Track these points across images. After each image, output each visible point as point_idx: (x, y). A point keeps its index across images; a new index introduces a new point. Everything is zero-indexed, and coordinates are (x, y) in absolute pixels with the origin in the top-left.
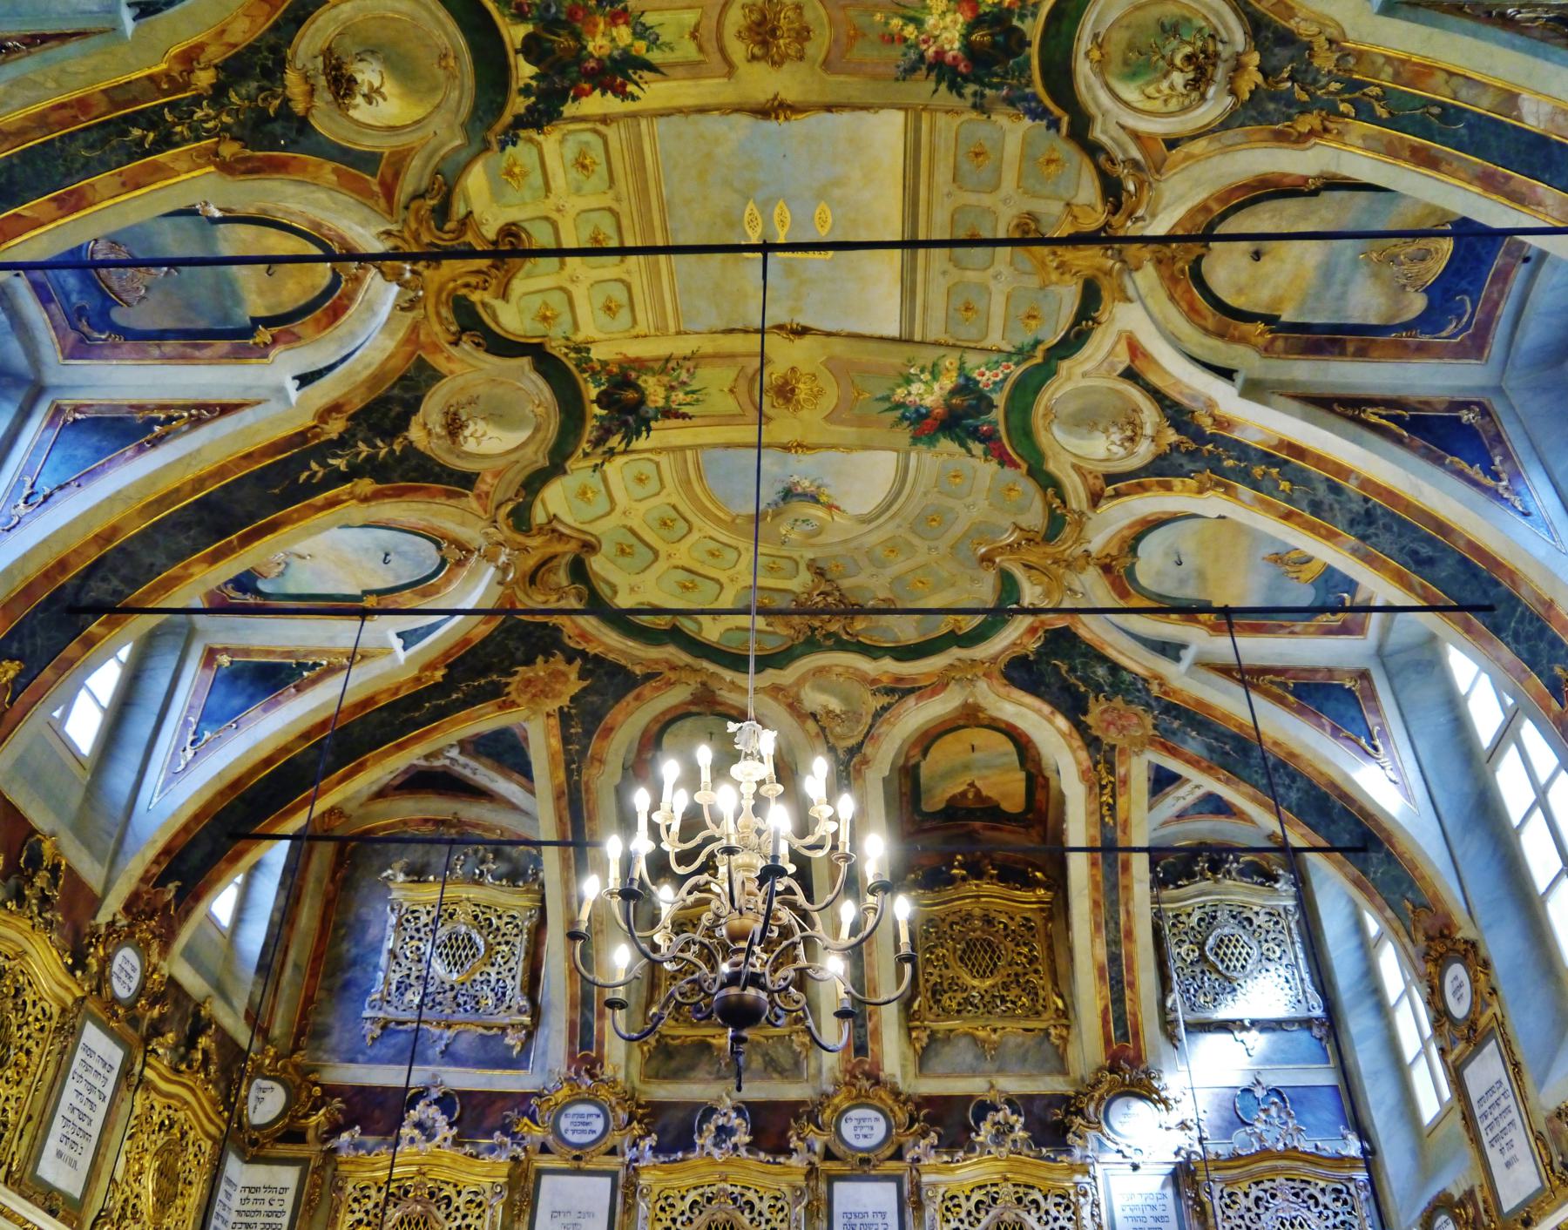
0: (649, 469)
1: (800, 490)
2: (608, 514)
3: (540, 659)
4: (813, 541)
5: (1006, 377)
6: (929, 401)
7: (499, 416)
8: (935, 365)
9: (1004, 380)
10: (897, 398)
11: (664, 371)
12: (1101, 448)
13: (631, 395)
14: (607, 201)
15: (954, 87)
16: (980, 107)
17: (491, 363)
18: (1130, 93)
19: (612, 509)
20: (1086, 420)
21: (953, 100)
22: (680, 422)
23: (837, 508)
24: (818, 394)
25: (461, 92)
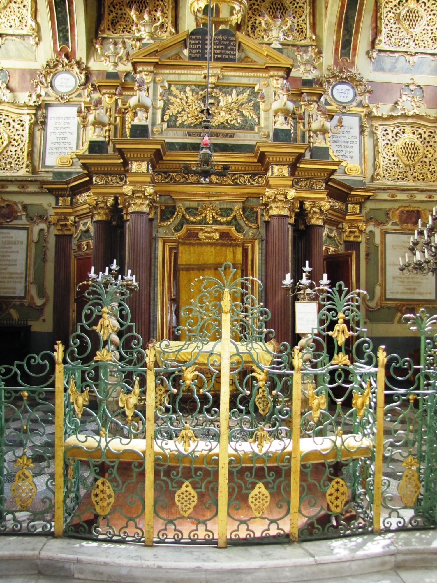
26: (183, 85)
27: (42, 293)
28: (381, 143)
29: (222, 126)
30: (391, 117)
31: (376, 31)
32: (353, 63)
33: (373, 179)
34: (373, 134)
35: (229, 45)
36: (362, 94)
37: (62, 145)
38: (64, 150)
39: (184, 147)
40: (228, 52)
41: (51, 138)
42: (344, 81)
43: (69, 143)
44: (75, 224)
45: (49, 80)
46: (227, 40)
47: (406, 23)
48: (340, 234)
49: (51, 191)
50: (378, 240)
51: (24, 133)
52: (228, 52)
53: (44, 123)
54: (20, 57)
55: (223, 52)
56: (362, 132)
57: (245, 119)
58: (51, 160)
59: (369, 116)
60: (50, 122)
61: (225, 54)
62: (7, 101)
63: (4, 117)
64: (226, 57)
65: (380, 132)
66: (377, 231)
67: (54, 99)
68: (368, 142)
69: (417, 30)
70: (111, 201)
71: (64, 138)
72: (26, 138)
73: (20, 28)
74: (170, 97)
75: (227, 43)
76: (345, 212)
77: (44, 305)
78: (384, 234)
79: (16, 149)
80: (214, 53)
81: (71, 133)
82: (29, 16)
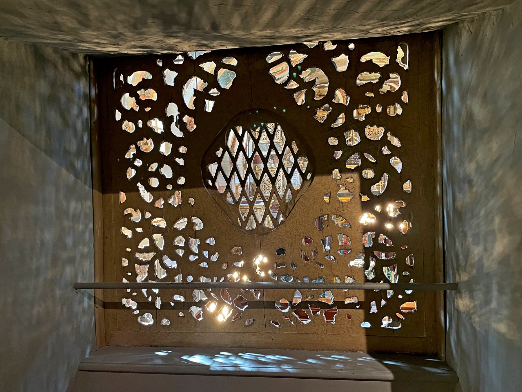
35: (357, 158)
37: (294, 182)
38: (295, 184)
40: (356, 161)
43: (297, 181)
45: (288, 158)
46: (356, 157)
51: (281, 178)
52: (356, 161)
55: (355, 161)
61: (355, 162)
62: (274, 167)
63: (273, 173)
64: (356, 163)
67: (290, 165)
71: (295, 179)
73: (276, 139)
74: (337, 177)
75: (356, 157)
79: (278, 184)
80: (352, 162)
81: (297, 177)
82: (279, 135)
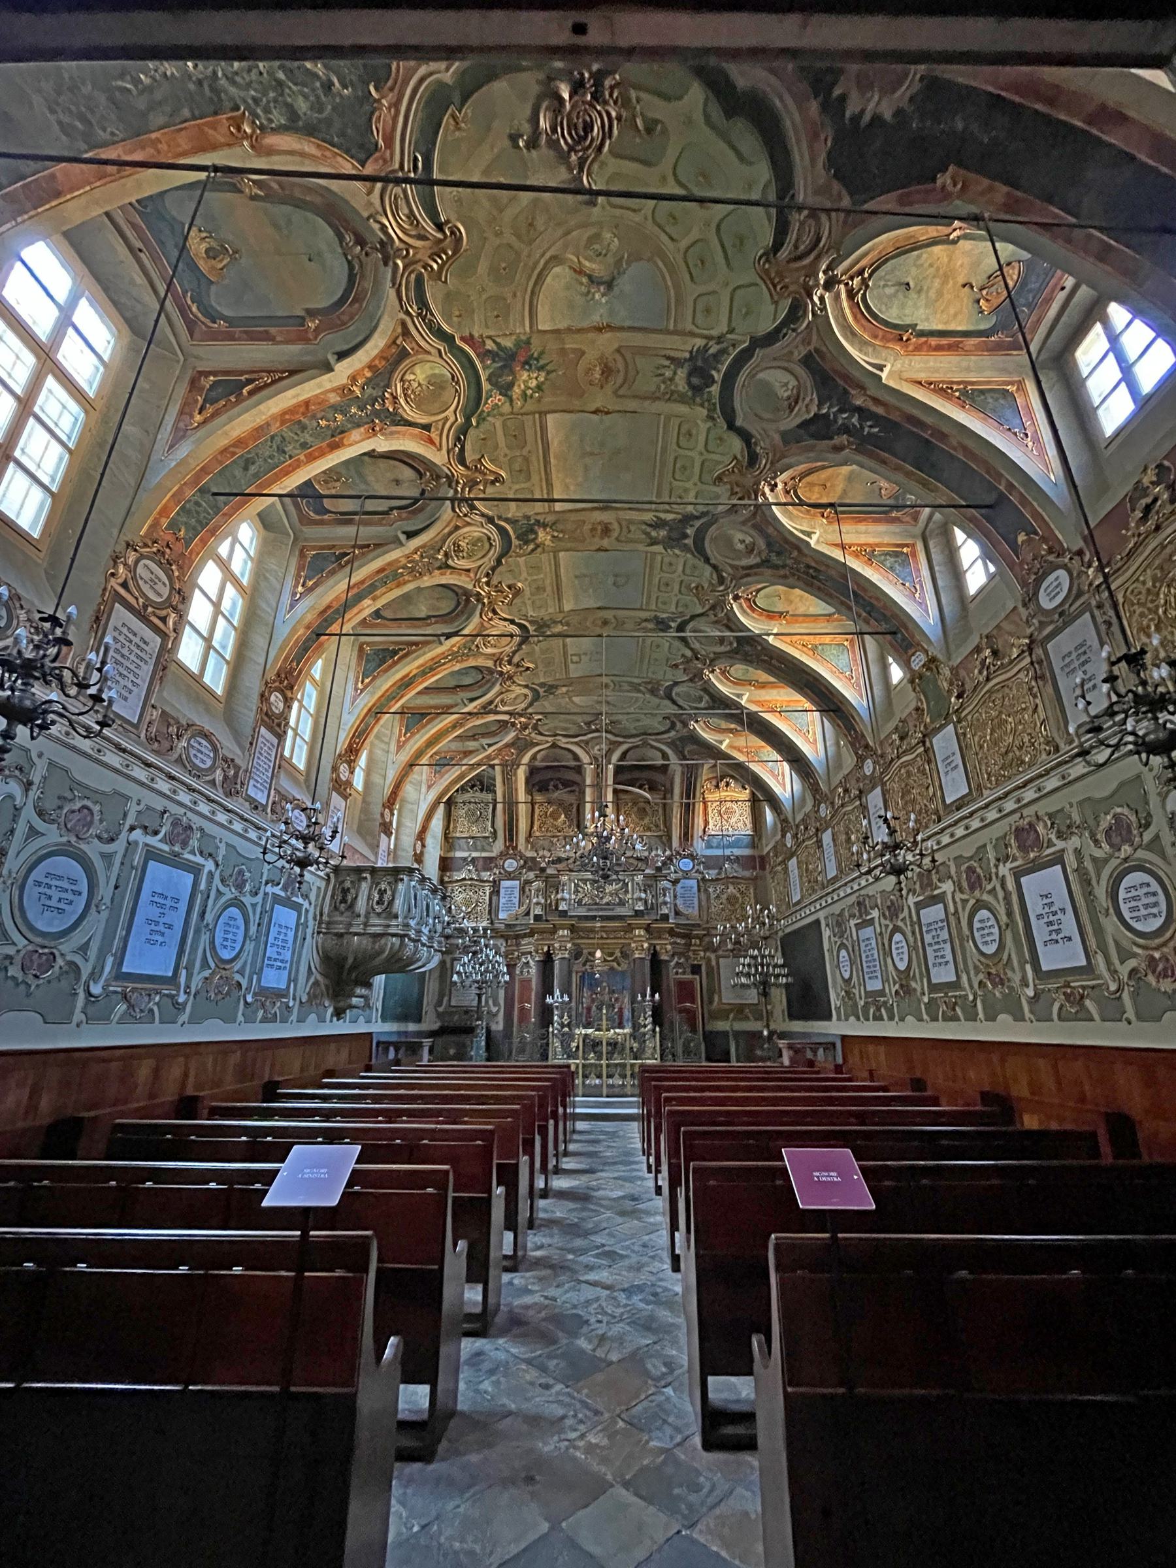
0: (700, 319)
1: (602, 288)
2: (739, 287)
3: (867, 118)
4: (591, 231)
5: (486, 403)
6: (525, 375)
7: (766, 391)
8: (526, 400)
9: (487, 399)
10: (543, 374)
11: (673, 392)
12: (419, 375)
13: (695, 381)
14: (675, 483)
15: (538, 521)
16: (528, 518)
17: (754, 429)
18: (476, 534)
19: (735, 290)
20: (437, 385)
21: (538, 517)
22: (672, 354)
23: (575, 270)
24: (589, 371)
25: (712, 531)
26: (585, 881)
27: (496, 1004)
28: (713, 896)
29: (608, 904)
30: (717, 880)
31: (706, 823)
32: (692, 845)
33: (708, 922)
34: (706, 890)
36: (699, 864)
39: (586, 918)
41: (502, 901)
42: (685, 857)
44: (519, 958)
47: (725, 817)
48: (687, 959)
49: (502, 936)
50: (714, 963)
53: (498, 892)
54: (483, 850)
56: (699, 890)
57: (620, 899)
58: (502, 915)
59: (704, 879)
60: (502, 892)
65: (711, 890)
66: (713, 956)
68: (703, 896)
69: (733, 820)
70: (546, 949)
72: (487, 901)
76: (691, 945)
77: (498, 1011)
78: (718, 958)
